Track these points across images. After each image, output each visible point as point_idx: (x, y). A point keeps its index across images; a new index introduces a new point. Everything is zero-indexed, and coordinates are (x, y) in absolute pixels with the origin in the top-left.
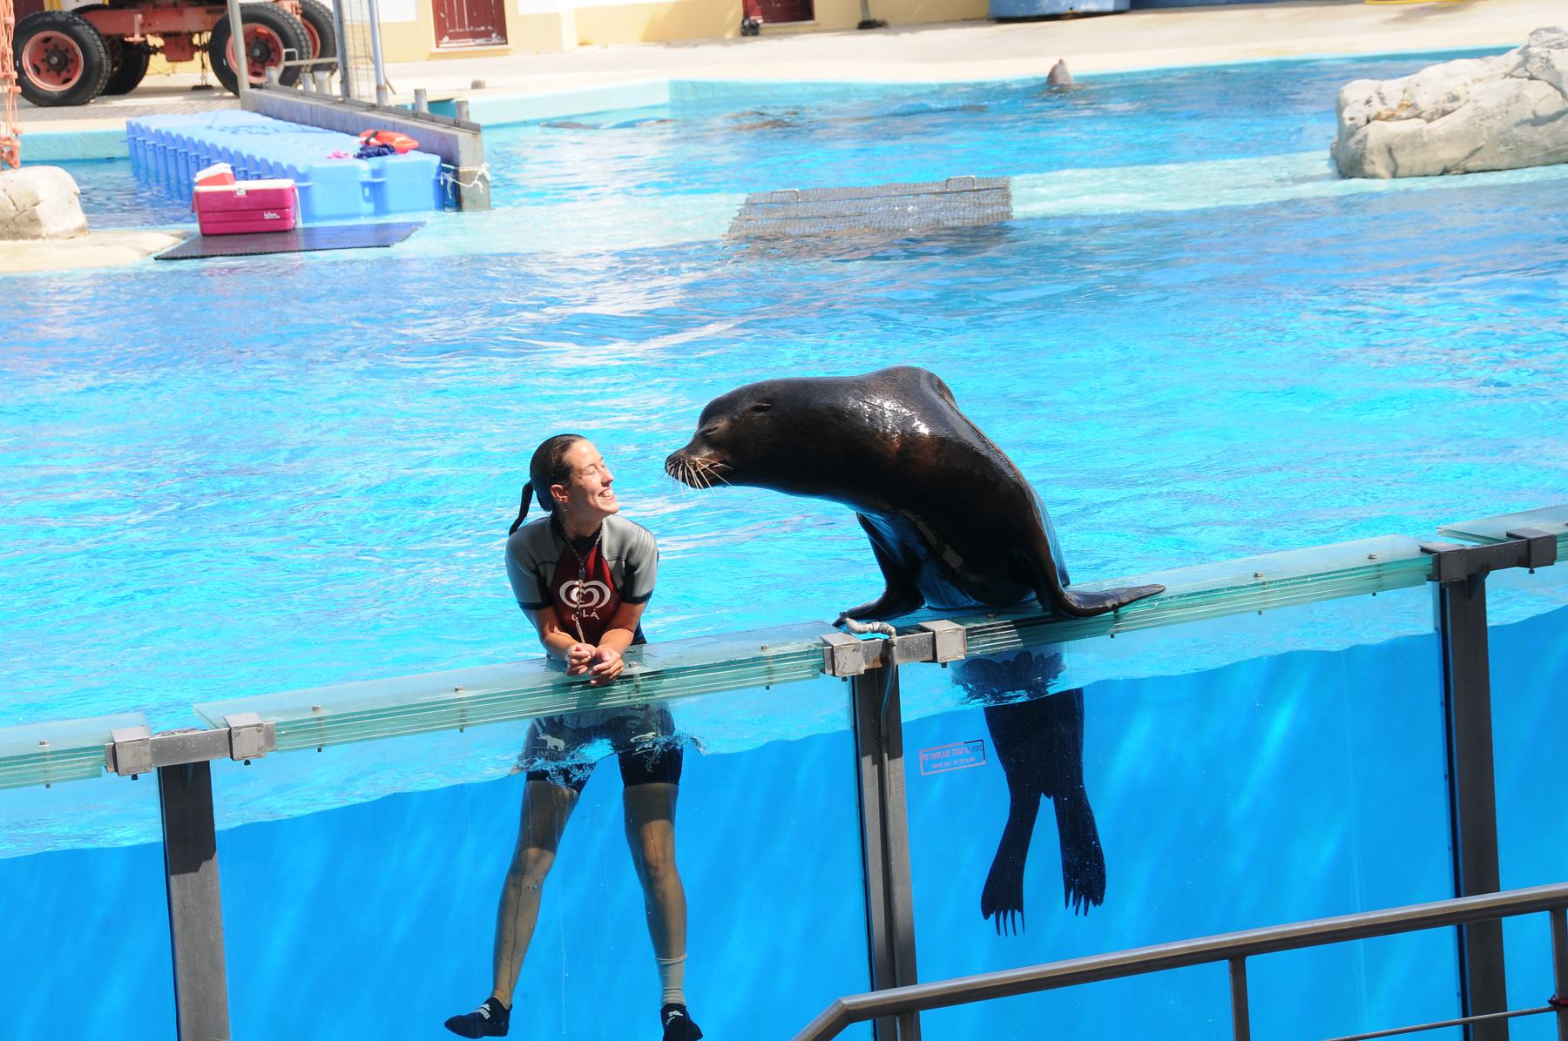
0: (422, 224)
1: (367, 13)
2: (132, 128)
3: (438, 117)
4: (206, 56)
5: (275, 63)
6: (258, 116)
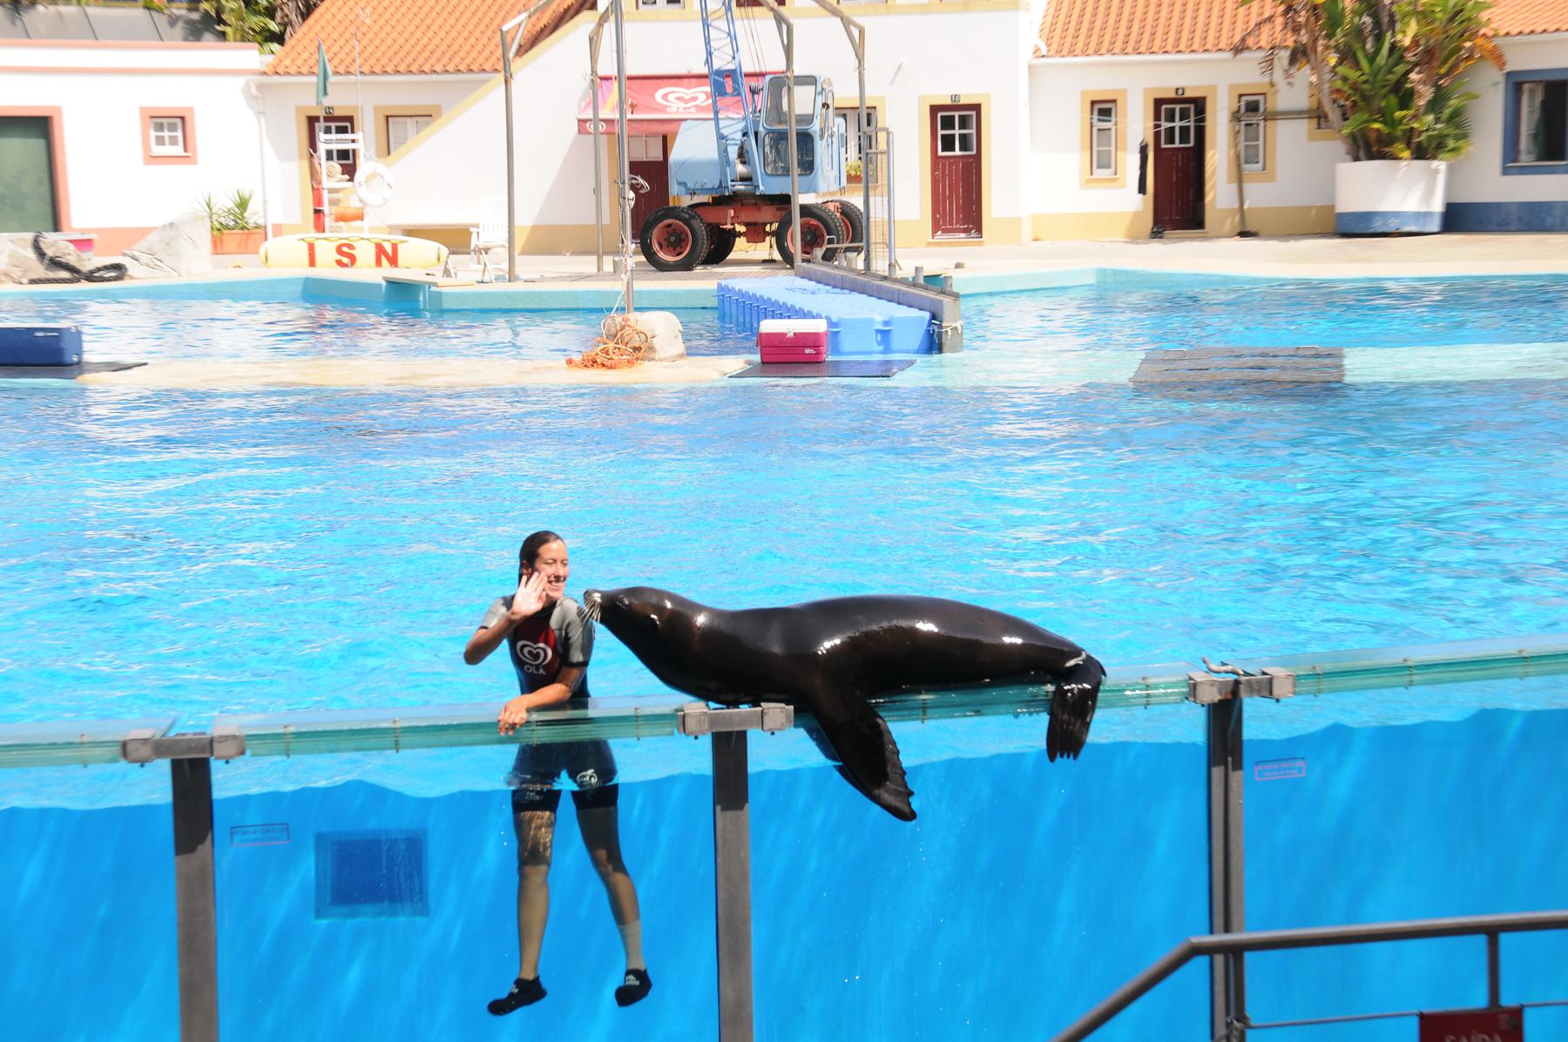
0: (911, 363)
1: (886, 212)
2: (720, 287)
3: (930, 286)
4: (774, 239)
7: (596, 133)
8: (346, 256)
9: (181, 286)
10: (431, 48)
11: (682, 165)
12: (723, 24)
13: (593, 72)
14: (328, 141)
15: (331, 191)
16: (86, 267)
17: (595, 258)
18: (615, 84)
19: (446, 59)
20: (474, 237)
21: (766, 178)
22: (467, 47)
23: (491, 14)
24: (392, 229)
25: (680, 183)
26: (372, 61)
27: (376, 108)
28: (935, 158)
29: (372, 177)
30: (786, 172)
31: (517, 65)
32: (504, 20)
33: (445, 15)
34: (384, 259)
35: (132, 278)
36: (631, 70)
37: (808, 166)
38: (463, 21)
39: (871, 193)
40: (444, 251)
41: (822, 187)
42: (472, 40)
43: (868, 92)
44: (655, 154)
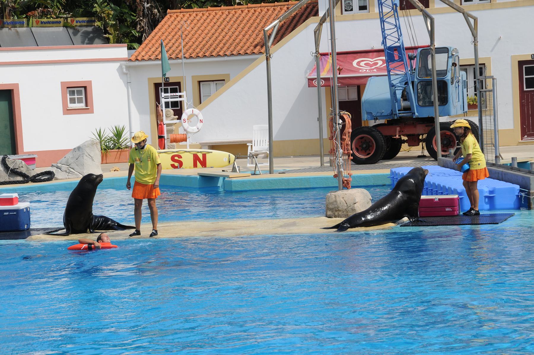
0: (512, 215)
1: (493, 126)
3: (521, 169)
4: (424, 144)
5: (453, 147)
6: (444, 169)
7: (319, 86)
8: (177, 163)
10: (224, 41)
11: (368, 102)
12: (392, 20)
13: (317, 51)
14: (165, 97)
15: (168, 125)
16: (32, 174)
17: (319, 158)
18: (330, 58)
19: (232, 48)
20: (249, 148)
21: (419, 108)
22: (245, 40)
23: (258, 21)
24: (202, 145)
25: (368, 113)
26: (190, 51)
27: (193, 77)
28: (522, 92)
29: (192, 115)
30: (432, 104)
31: (272, 49)
32: (265, 24)
33: (232, 22)
34: (198, 163)
35: (57, 179)
36: (338, 49)
37: (444, 100)
38: (241, 26)
39: (483, 115)
40: (233, 157)
41: (453, 112)
42: (247, 36)
43: (480, 55)
44: (353, 96)
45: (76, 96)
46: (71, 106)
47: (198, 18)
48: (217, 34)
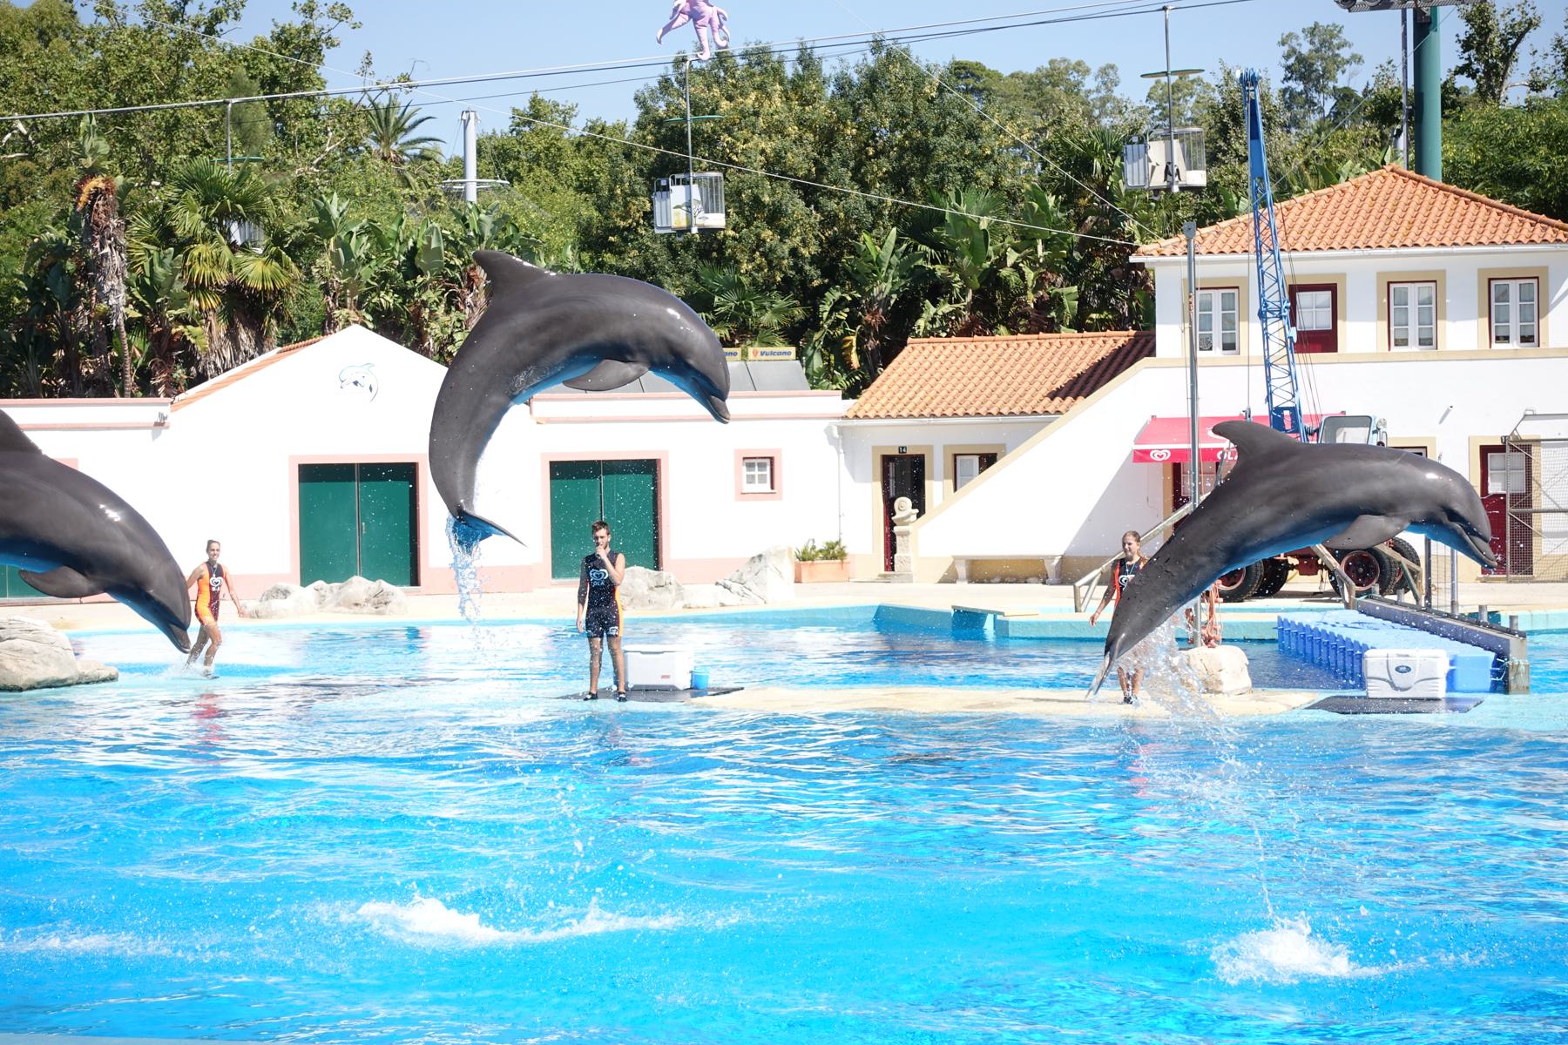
2: (1282, 622)
9: (767, 613)
10: (998, 391)
19: (1012, 402)
23: (1055, 360)
33: (1012, 361)
38: (1028, 367)
42: (1037, 385)
45: (756, 472)
46: (748, 488)
47: (957, 352)
48: (987, 380)
